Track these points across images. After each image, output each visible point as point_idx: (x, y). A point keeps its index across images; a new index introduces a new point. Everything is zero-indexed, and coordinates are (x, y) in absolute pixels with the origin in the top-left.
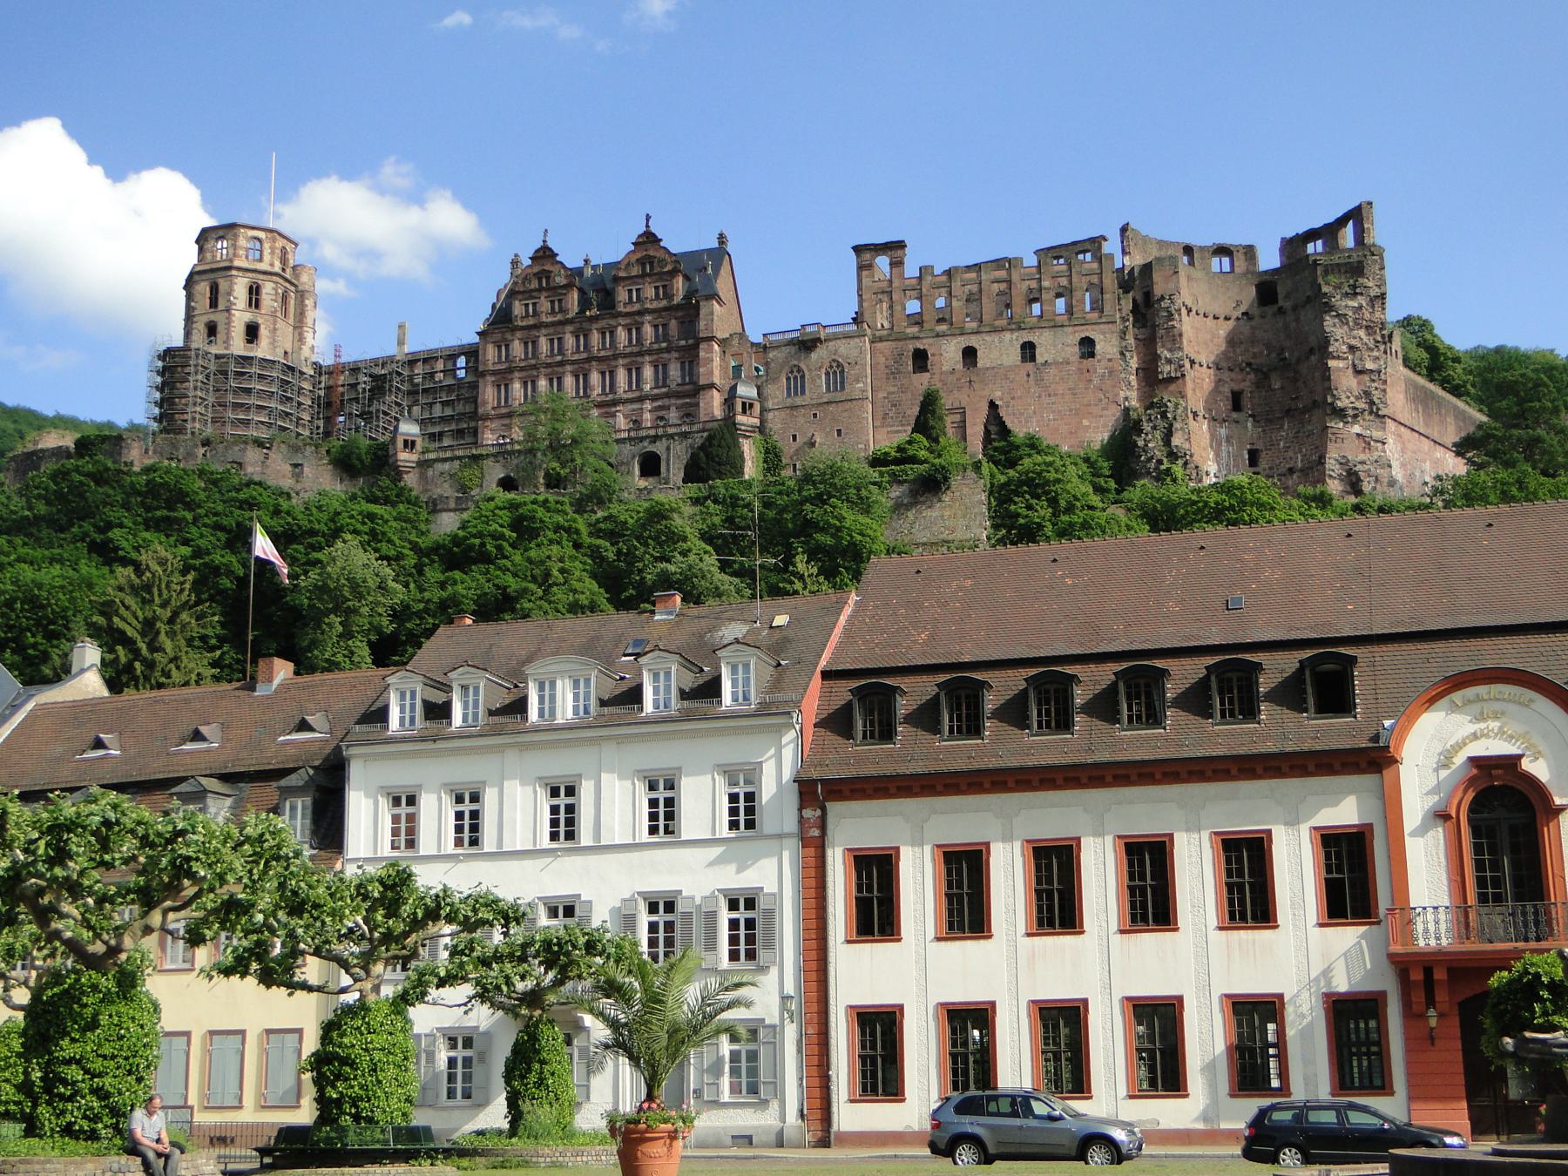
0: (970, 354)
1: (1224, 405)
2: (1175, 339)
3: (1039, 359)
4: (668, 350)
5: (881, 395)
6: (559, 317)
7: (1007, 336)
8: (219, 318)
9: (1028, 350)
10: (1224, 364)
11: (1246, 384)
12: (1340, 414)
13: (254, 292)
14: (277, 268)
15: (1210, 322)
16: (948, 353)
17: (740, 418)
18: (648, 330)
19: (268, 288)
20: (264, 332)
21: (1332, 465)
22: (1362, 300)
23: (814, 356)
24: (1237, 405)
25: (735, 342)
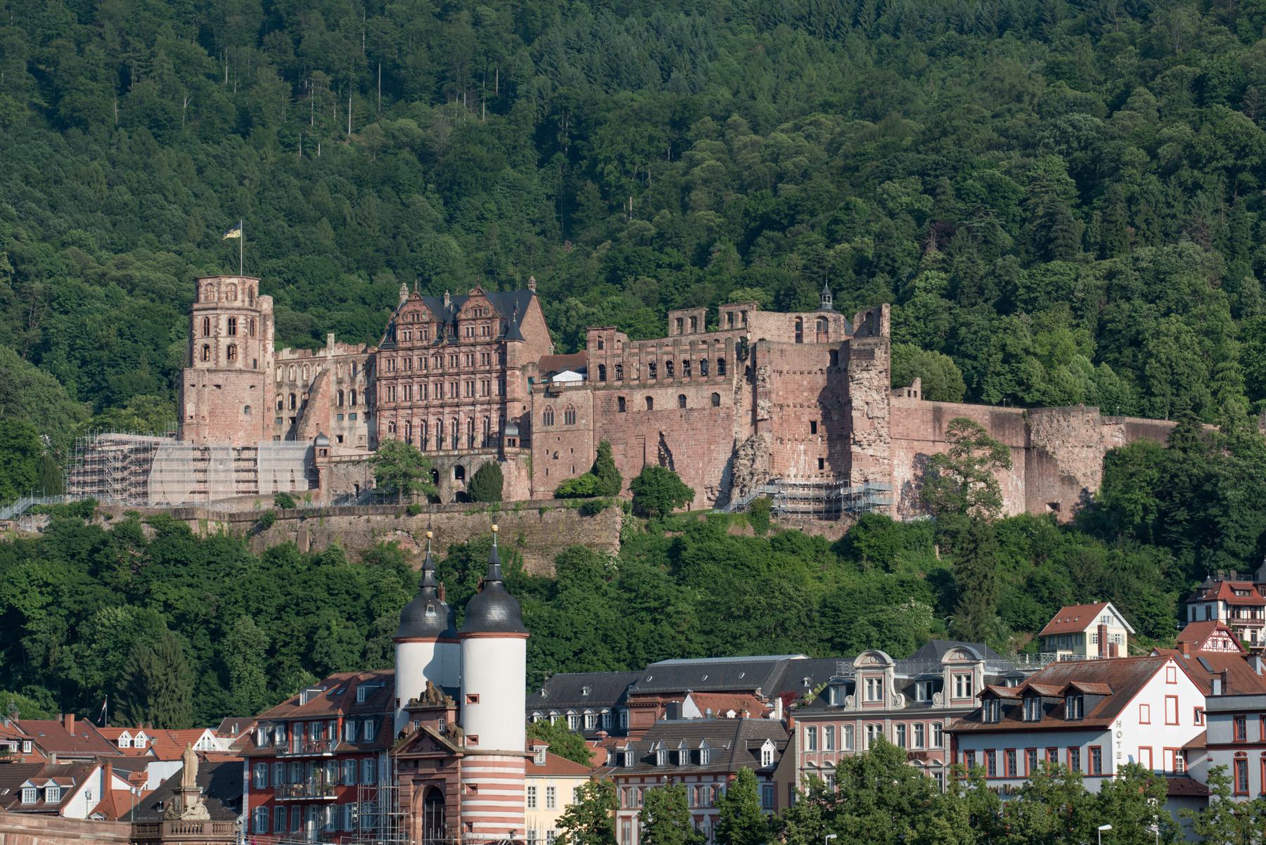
0: (649, 399)
1: (805, 429)
2: (767, 394)
3: (688, 406)
4: (489, 372)
5: (598, 425)
6: (425, 343)
7: (670, 391)
8: (211, 341)
9: (683, 398)
10: (806, 404)
11: (819, 418)
12: (859, 443)
13: (232, 322)
14: (247, 304)
15: (798, 377)
16: (637, 400)
17: (507, 449)
18: (478, 356)
19: (241, 321)
20: (240, 350)
21: (855, 474)
22: (873, 373)
23: (559, 400)
24: (814, 431)
25: (530, 368)
